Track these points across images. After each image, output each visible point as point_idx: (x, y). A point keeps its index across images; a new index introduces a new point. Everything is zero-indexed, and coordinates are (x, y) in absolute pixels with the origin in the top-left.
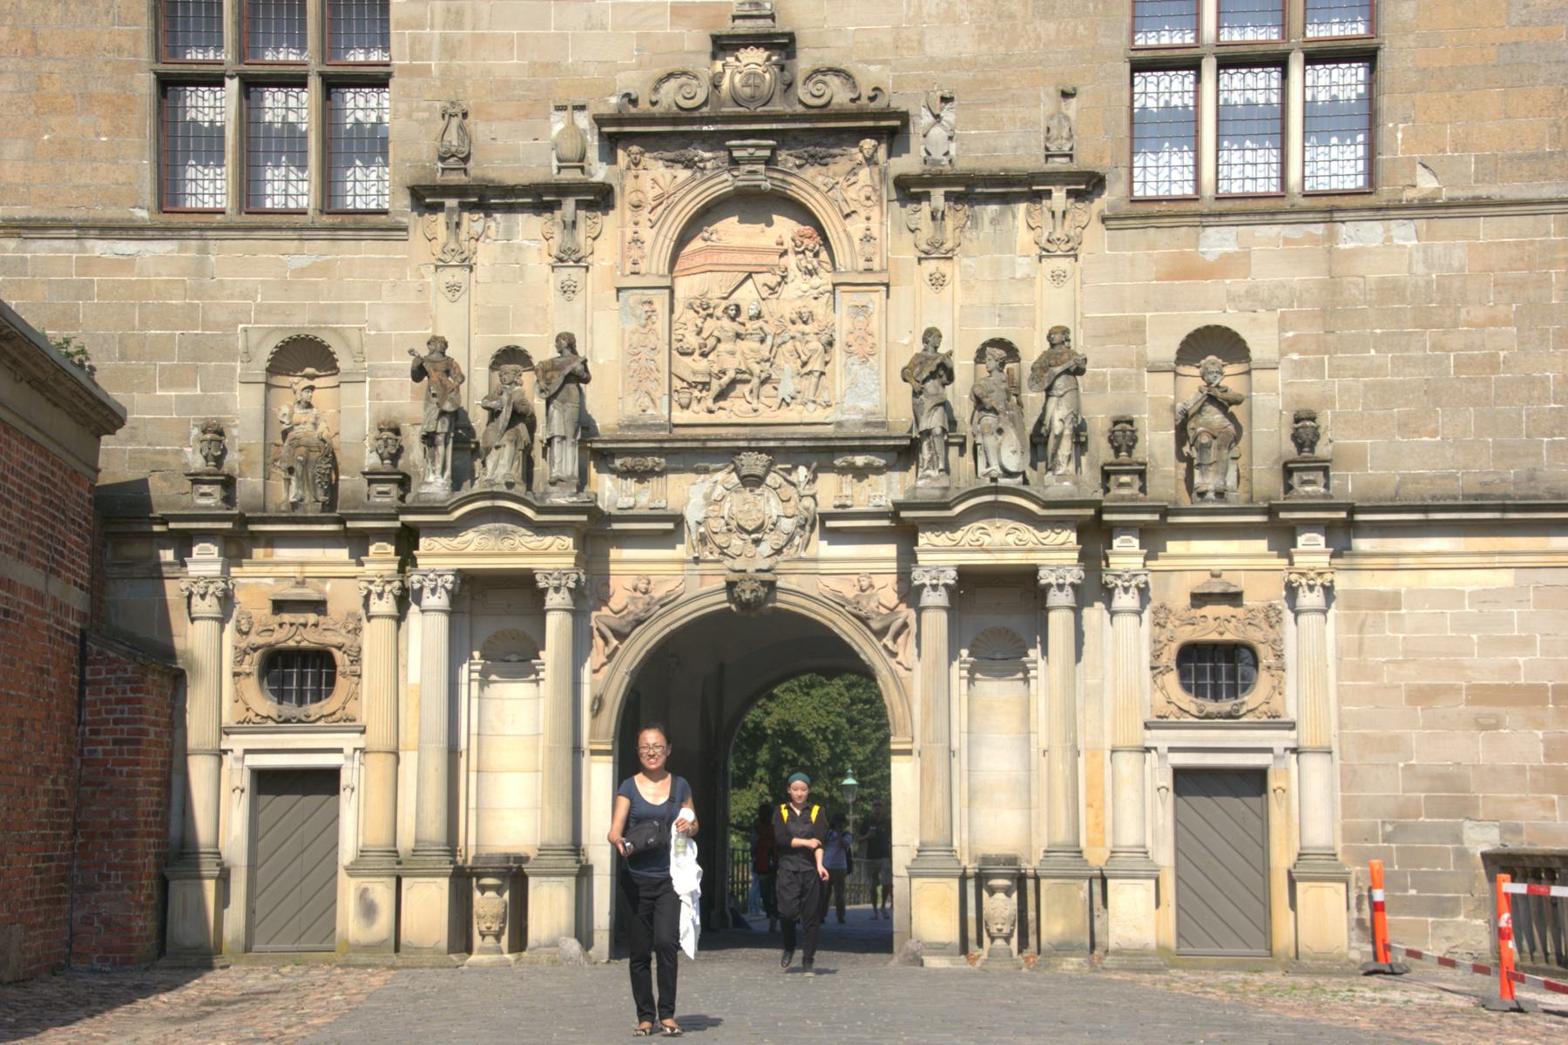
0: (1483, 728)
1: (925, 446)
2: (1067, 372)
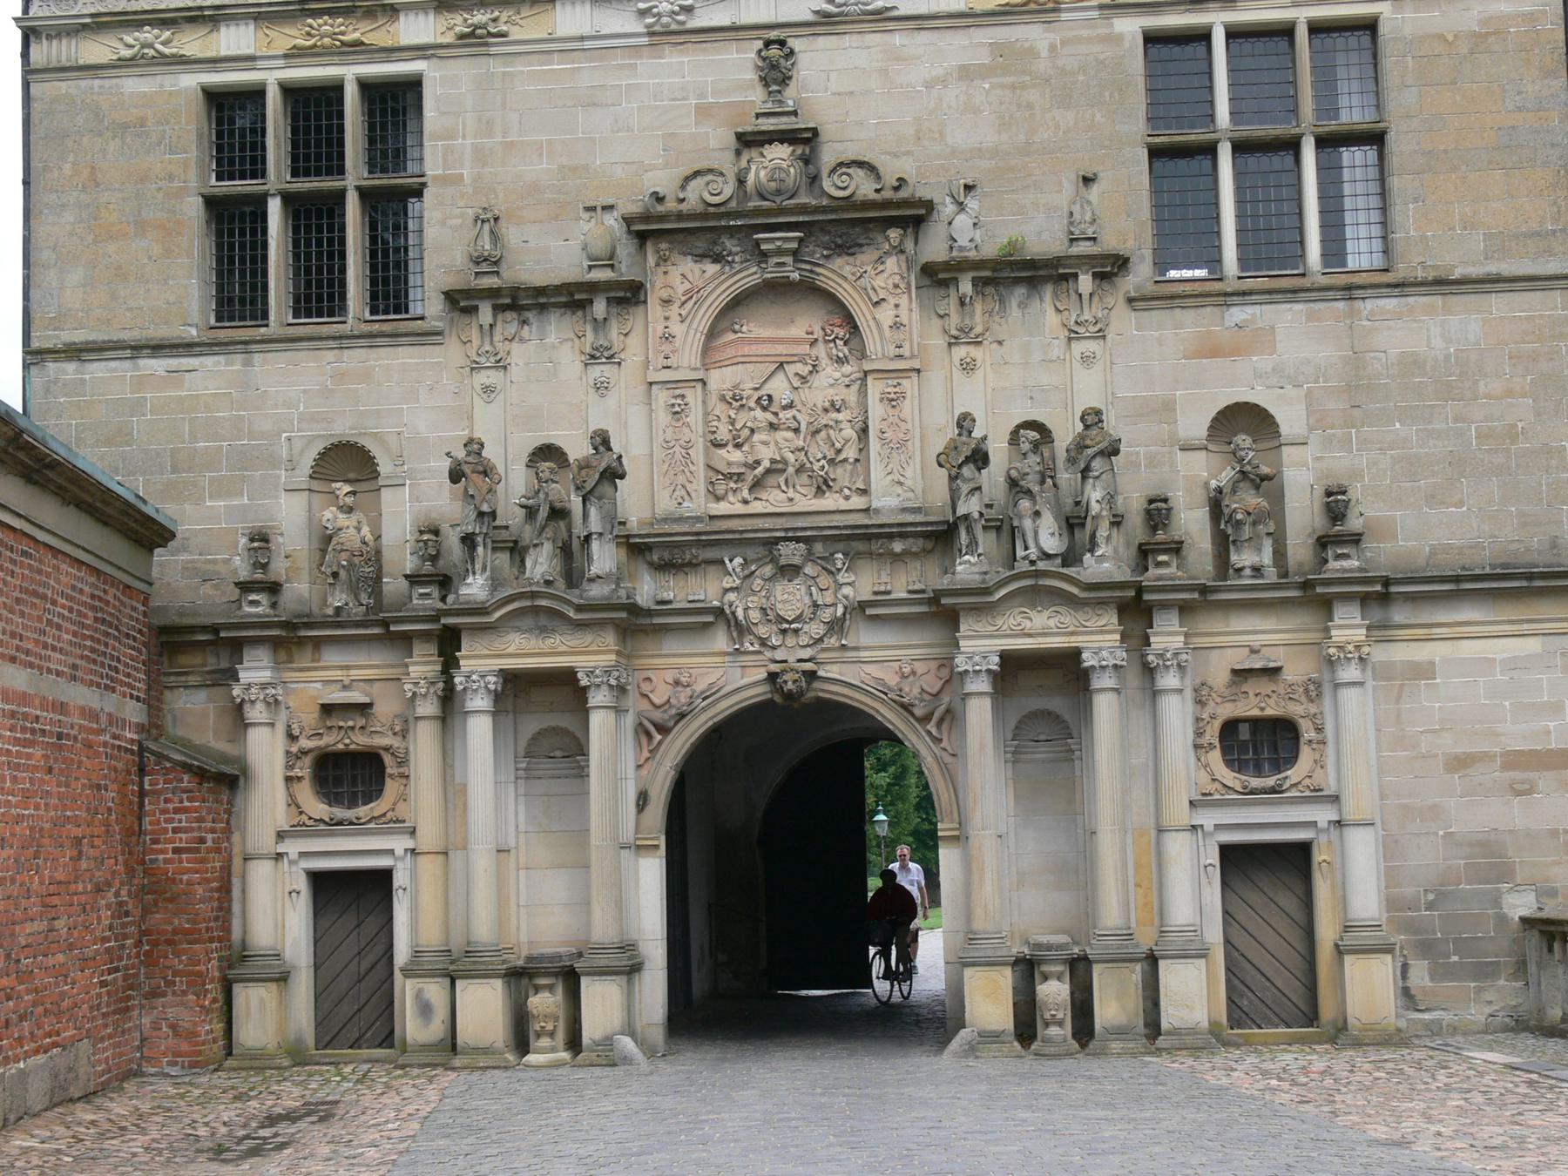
0: (1518, 793)
2: (1101, 453)
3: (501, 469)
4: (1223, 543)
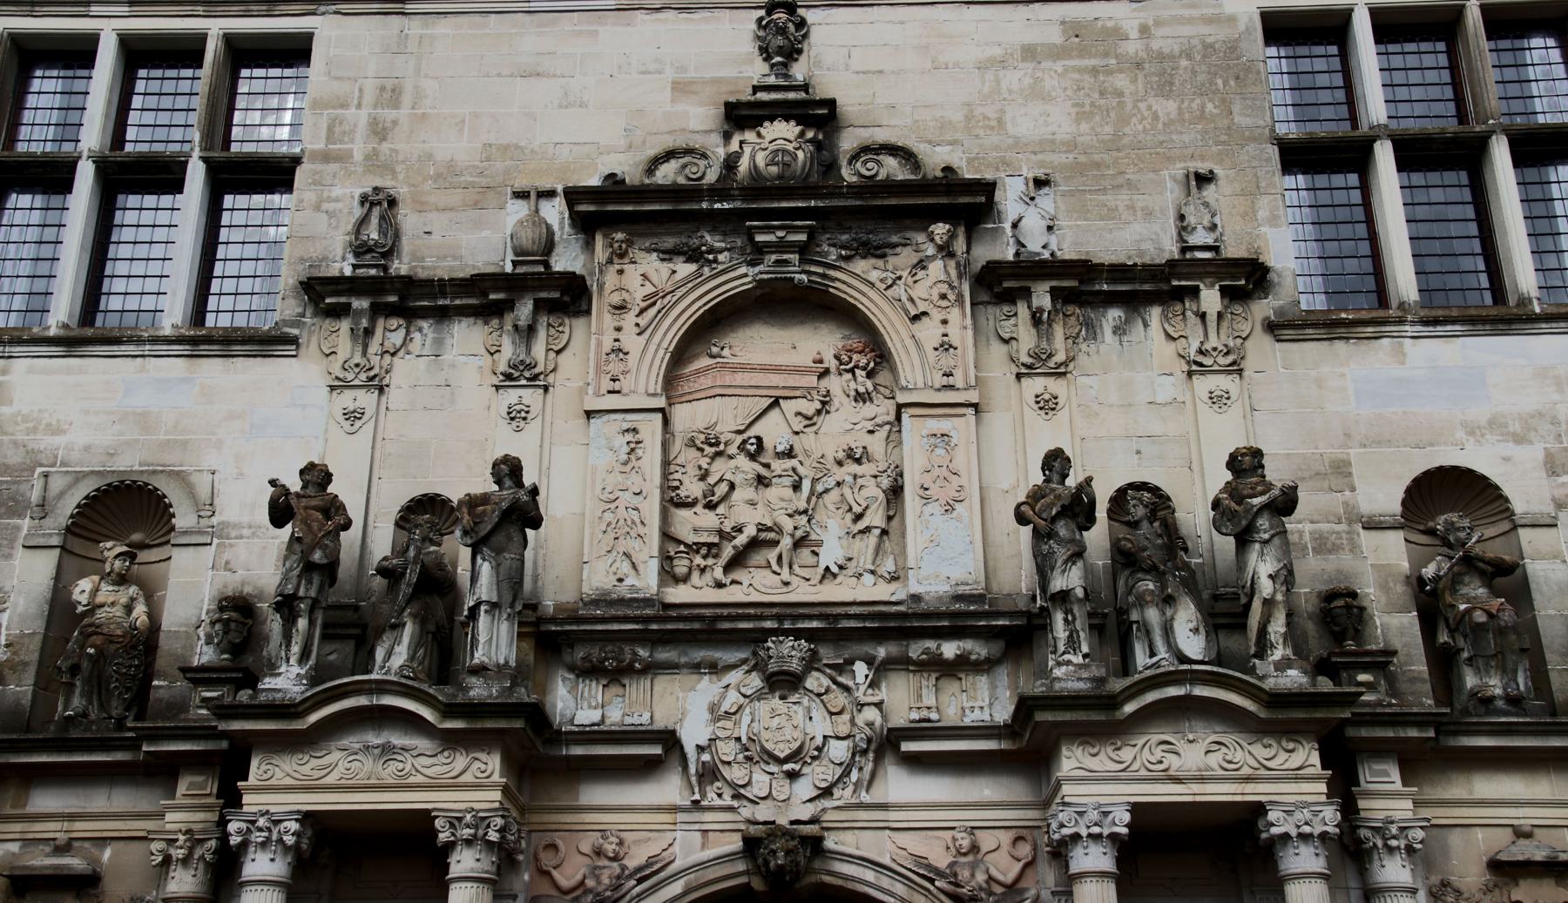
1: (1059, 618)
3: (355, 512)
4: (1443, 663)
